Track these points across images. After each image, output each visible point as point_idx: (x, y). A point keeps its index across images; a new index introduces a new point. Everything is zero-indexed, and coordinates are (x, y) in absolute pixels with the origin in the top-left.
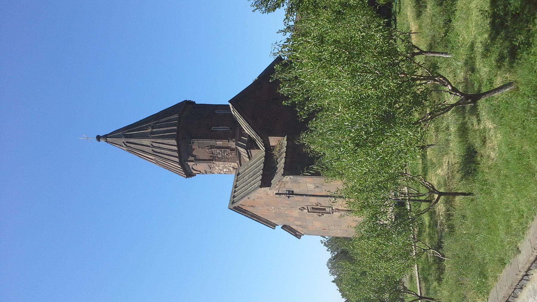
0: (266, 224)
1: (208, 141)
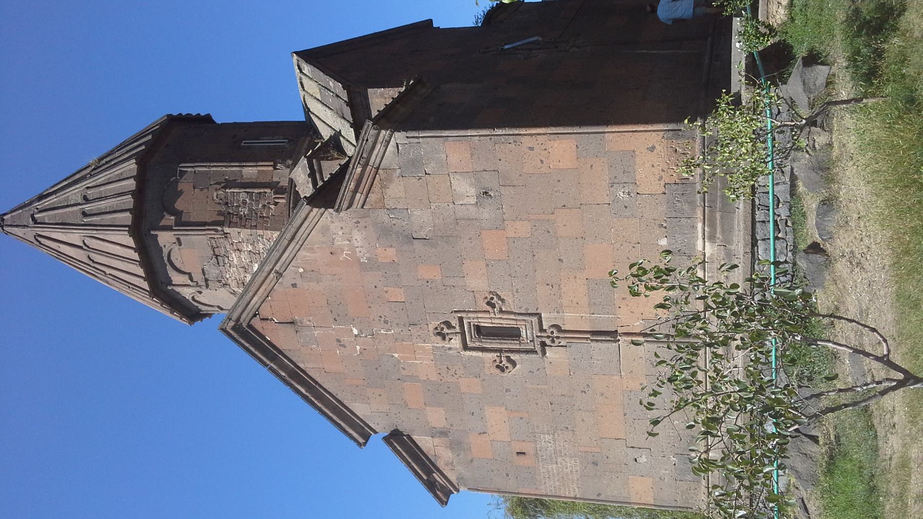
0: (335, 418)
1: (219, 169)
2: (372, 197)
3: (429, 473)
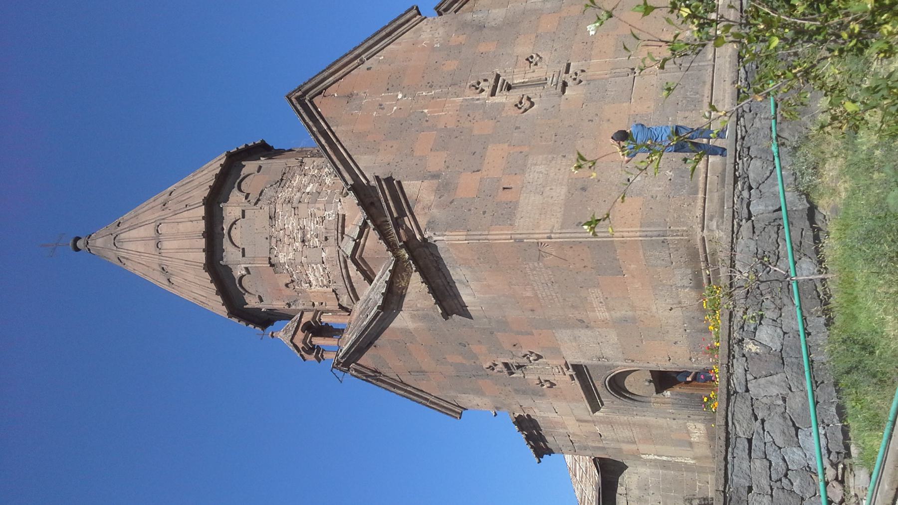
2: (466, 6)
3: (402, 214)
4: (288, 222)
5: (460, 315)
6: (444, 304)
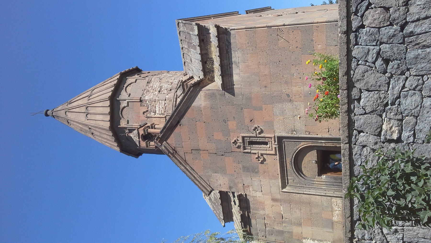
4: (155, 84)
5: (229, 93)
6: (224, 78)
